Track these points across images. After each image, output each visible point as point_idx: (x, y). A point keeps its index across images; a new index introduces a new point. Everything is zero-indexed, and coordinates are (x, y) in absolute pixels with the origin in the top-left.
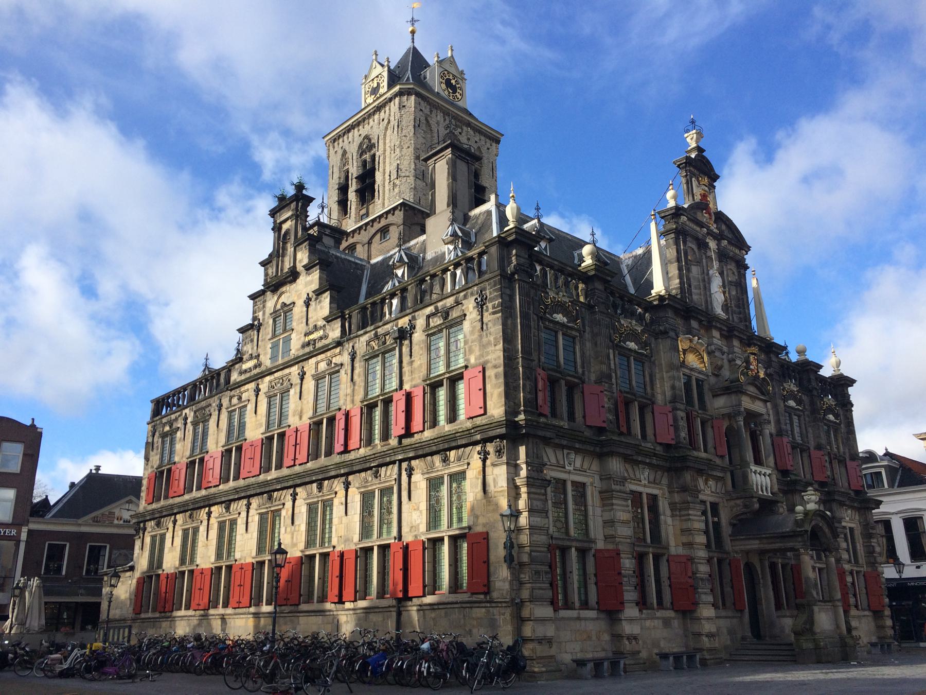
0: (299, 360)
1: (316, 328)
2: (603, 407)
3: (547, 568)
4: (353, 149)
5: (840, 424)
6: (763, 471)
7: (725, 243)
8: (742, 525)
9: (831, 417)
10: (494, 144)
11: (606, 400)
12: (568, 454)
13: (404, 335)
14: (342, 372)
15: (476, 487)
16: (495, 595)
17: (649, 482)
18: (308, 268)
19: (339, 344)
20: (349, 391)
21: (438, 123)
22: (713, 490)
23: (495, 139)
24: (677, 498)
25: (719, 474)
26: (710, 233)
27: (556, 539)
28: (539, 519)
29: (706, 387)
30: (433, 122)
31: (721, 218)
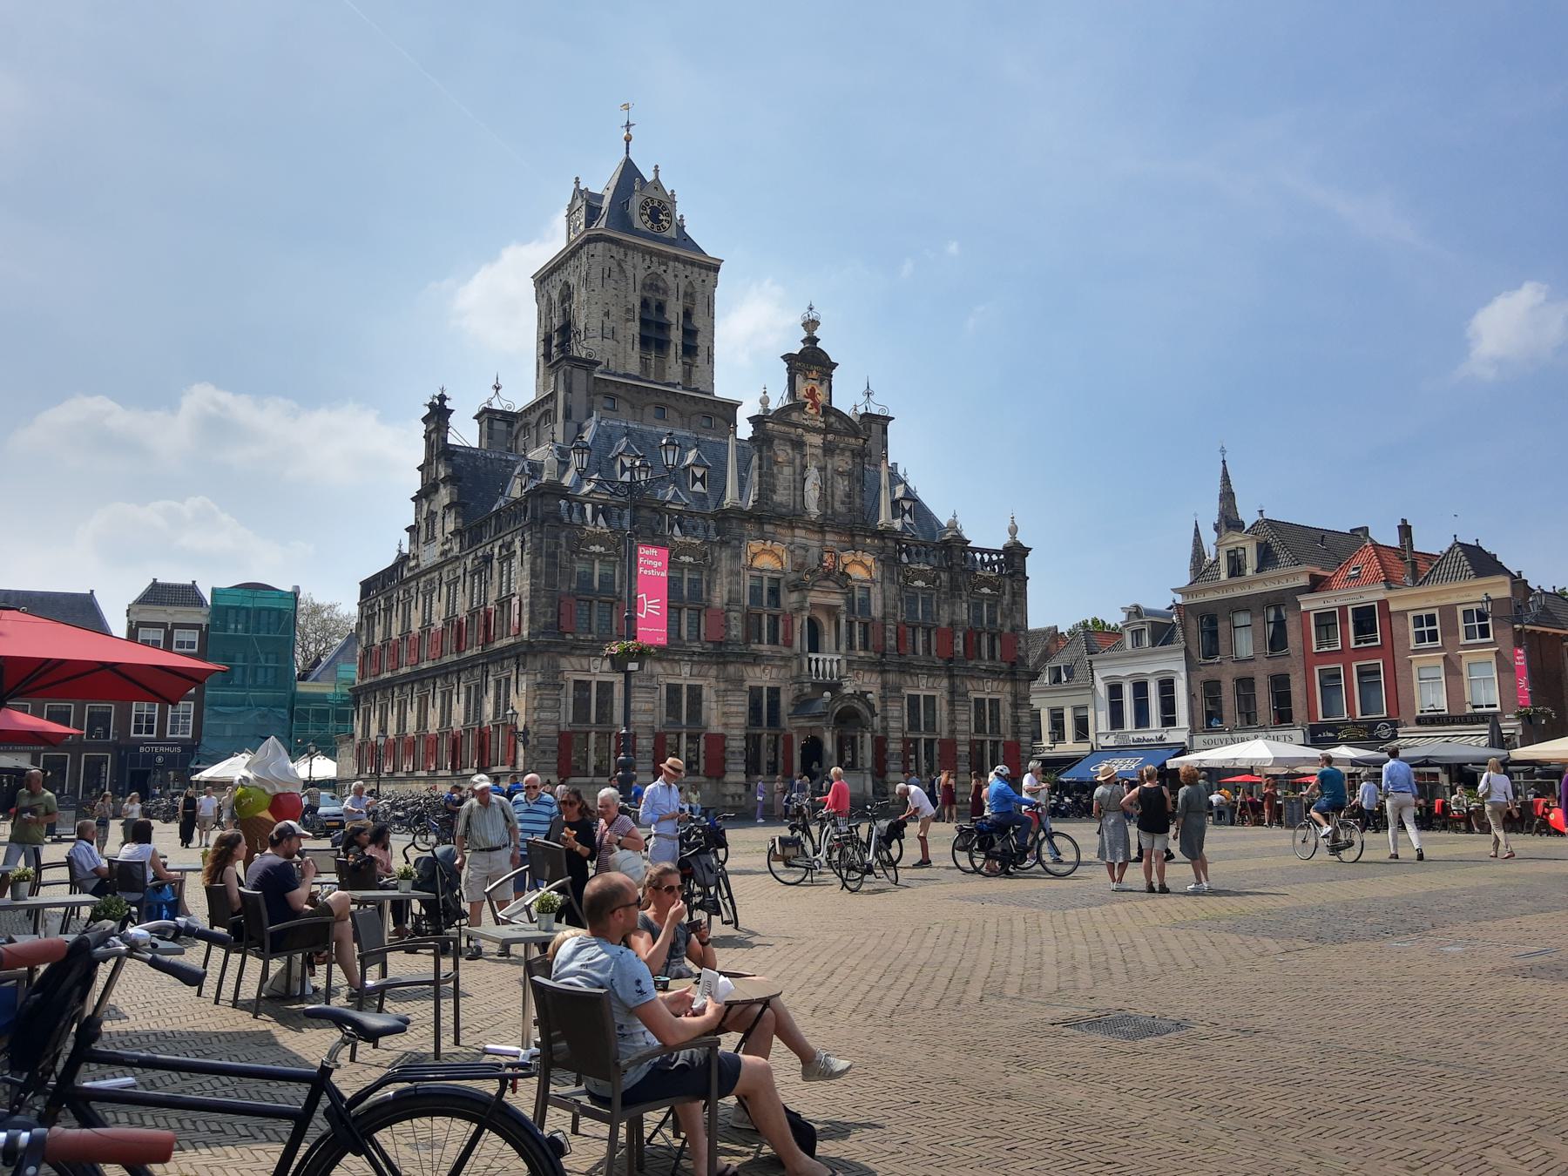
0: (438, 567)
1: (447, 540)
4: (555, 296)
7: (830, 437)
8: (802, 705)
10: (712, 274)
13: (488, 559)
18: (444, 481)
19: (457, 558)
21: (634, 267)
23: (714, 267)
24: (722, 686)
26: (807, 429)
29: (782, 583)
30: (628, 267)
31: (828, 410)
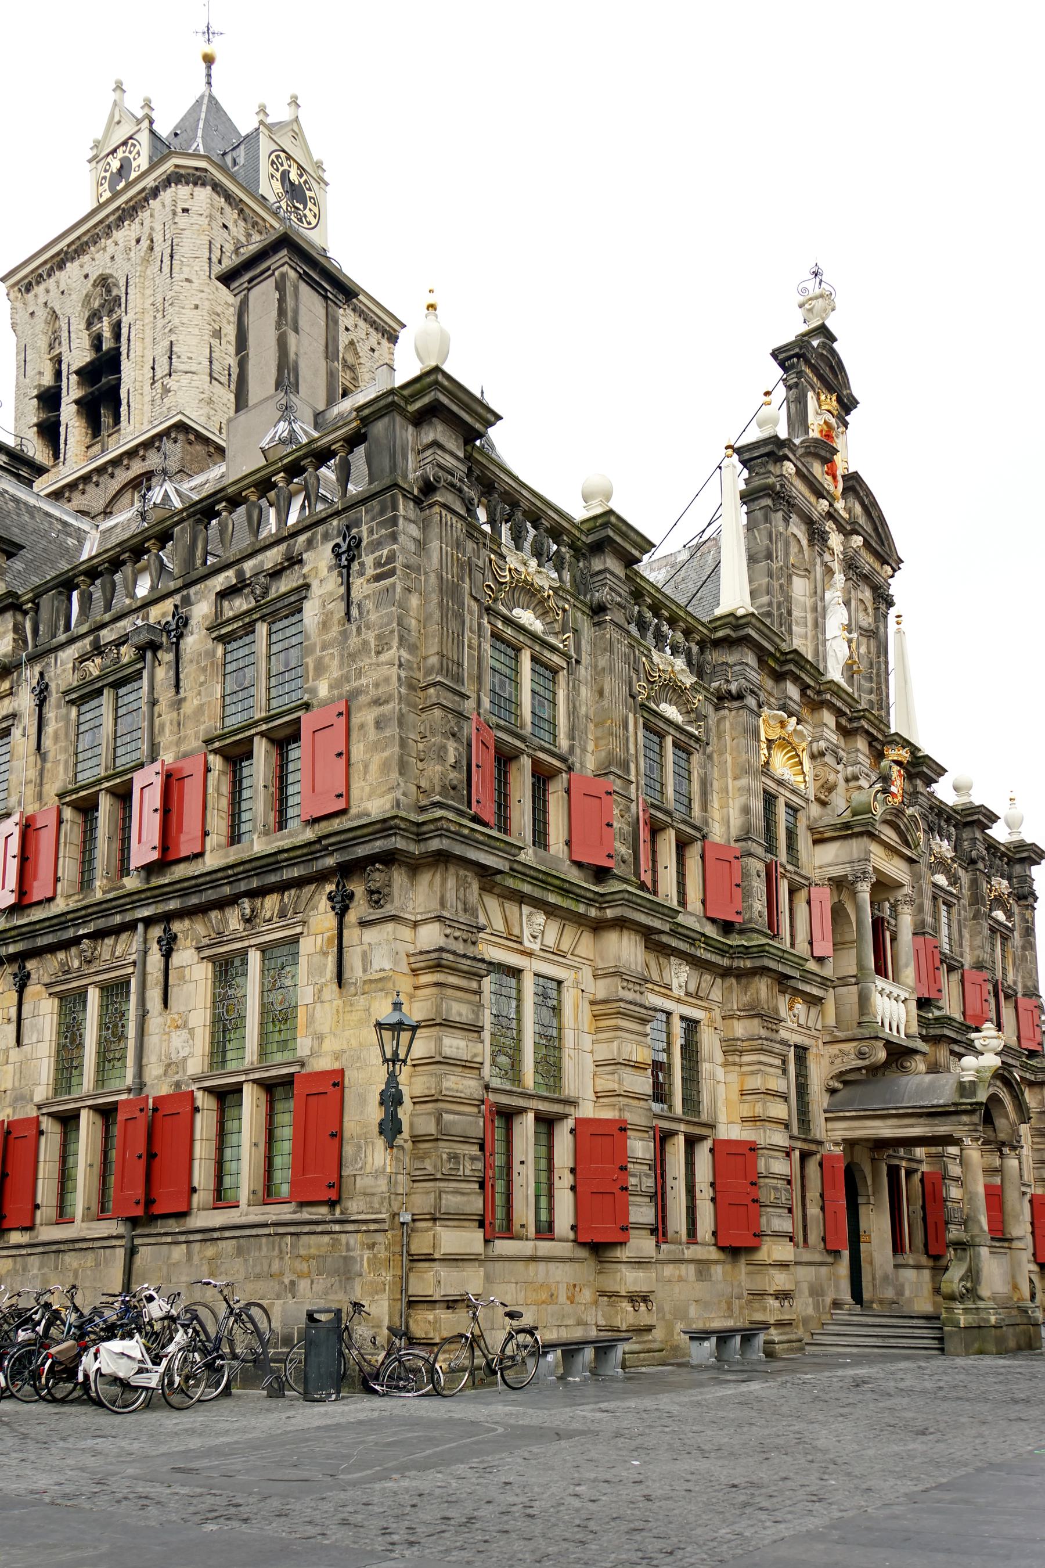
2: (610, 825)
3: (475, 1151)
4: (74, 313)
5: (1012, 930)
6: (896, 992)
9: (1000, 915)
11: (616, 812)
12: (531, 914)
14: (16, 732)
15: (322, 973)
16: (355, 1207)
17: (688, 994)
20: (32, 774)
22: (802, 1021)
25: (815, 991)
27: (497, 1091)
28: (462, 1044)
